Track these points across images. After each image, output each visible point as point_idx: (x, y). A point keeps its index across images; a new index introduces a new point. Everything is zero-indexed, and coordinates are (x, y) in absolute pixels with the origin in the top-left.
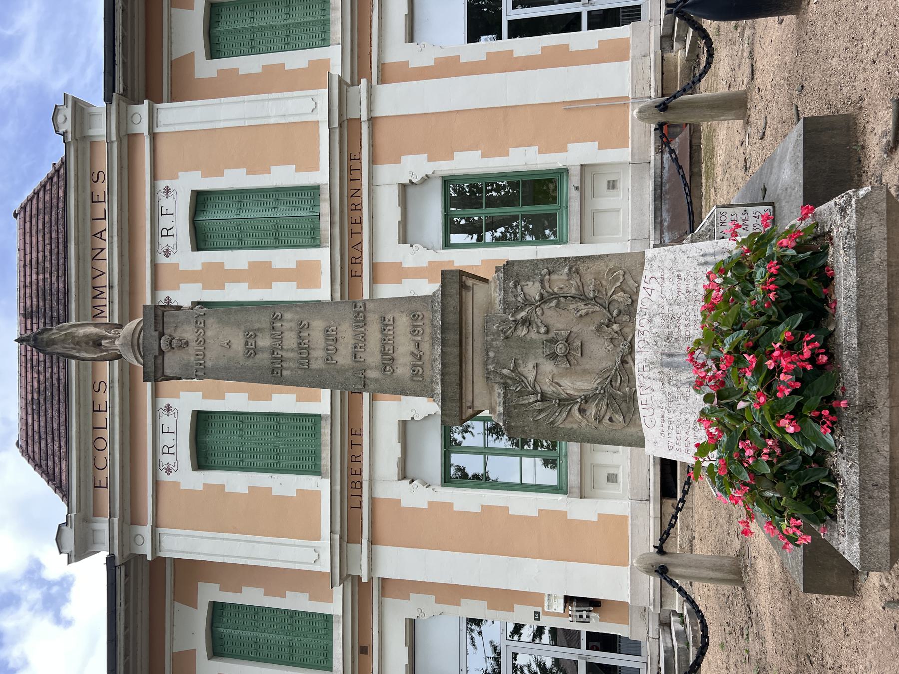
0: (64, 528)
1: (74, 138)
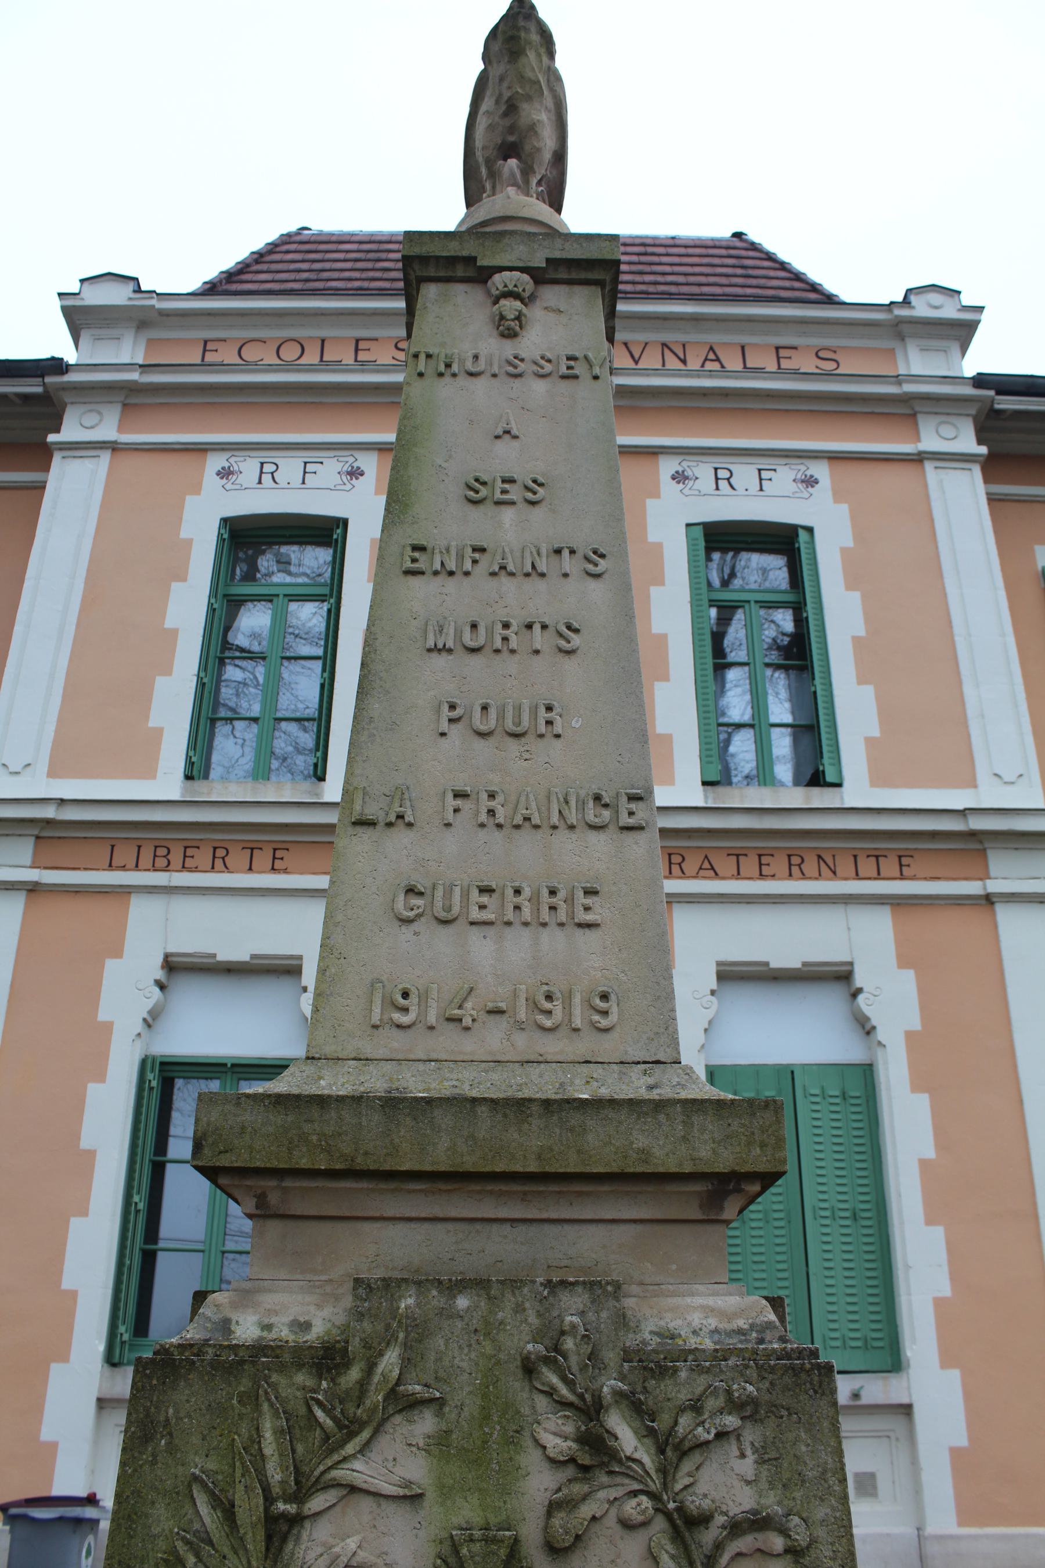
0: (131, 286)
1: (900, 322)
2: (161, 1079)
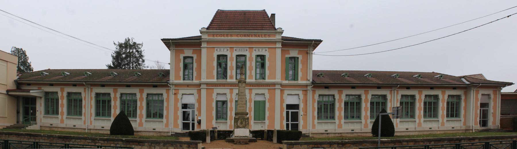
2: (217, 102)
